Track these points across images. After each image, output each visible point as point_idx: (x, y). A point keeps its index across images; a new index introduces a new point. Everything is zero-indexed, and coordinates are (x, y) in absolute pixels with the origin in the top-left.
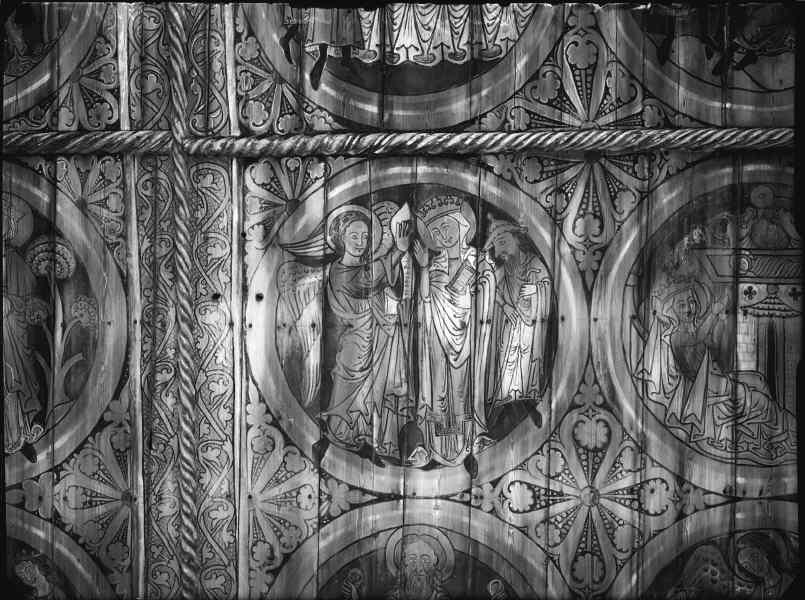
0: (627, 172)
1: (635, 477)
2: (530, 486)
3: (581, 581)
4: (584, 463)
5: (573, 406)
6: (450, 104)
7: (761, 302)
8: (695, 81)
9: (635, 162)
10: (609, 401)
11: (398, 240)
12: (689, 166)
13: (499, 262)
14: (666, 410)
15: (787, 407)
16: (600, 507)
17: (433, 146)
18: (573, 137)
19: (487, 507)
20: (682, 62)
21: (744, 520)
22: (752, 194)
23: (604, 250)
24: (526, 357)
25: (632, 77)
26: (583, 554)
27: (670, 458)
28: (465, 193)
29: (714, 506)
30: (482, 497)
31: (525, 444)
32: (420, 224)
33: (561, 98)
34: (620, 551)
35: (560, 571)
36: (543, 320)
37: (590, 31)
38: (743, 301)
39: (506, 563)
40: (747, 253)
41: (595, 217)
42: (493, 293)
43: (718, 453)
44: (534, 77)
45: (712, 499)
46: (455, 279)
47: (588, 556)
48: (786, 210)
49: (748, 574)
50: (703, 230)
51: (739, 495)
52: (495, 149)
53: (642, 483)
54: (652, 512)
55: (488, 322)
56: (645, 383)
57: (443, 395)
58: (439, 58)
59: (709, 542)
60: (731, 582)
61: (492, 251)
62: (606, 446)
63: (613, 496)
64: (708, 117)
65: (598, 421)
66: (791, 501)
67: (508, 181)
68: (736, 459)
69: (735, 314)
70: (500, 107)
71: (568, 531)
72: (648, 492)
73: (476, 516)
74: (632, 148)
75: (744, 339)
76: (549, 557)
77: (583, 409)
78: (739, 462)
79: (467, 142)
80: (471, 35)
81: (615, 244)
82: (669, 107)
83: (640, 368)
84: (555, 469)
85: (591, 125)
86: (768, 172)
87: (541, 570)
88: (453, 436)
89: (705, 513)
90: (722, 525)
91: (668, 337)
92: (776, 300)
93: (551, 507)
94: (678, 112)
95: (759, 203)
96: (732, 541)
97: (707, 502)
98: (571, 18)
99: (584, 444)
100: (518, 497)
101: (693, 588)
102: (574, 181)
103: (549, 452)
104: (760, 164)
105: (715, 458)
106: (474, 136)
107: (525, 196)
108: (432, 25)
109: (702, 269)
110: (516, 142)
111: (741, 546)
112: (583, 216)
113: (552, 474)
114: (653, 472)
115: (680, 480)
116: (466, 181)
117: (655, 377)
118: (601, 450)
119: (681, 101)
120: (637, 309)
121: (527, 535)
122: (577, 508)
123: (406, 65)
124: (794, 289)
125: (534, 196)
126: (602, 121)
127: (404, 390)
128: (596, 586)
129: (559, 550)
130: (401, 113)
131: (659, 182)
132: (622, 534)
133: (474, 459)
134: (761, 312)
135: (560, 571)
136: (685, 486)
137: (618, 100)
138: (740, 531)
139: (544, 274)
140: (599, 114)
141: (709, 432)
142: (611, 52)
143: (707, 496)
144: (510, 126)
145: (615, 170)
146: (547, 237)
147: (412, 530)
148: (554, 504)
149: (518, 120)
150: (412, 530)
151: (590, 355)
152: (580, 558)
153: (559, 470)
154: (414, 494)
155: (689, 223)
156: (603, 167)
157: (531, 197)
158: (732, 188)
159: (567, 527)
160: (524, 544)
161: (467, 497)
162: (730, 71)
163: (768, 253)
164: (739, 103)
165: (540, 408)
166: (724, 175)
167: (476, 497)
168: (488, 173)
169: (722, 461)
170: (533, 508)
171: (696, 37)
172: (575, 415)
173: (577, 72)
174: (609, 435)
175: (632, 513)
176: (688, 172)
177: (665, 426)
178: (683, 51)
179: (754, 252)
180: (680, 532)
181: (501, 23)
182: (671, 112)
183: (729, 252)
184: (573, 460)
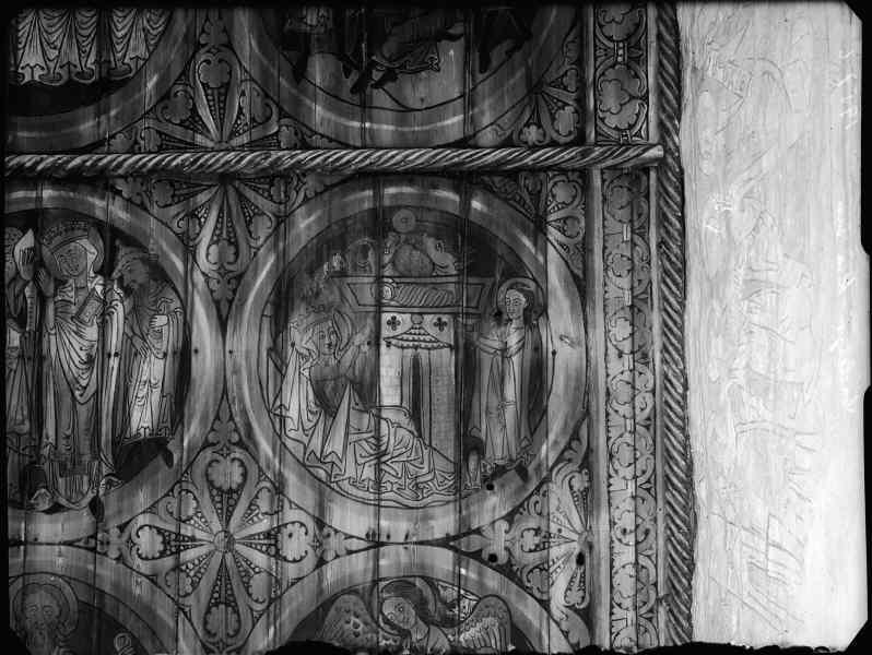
0: (262, 195)
1: (272, 520)
2: (159, 531)
3: (215, 635)
4: (219, 505)
5: (207, 445)
6: (79, 124)
7: (405, 333)
8: (333, 99)
9: (272, 185)
10: (244, 439)
11: (22, 269)
12: (327, 188)
13: (128, 291)
16: (236, 555)
17: (55, 167)
18: (199, 158)
19: (114, 554)
20: (318, 81)
21: (390, 566)
22: (394, 219)
23: (239, 277)
24: (157, 393)
25: (267, 96)
26: (216, 605)
27: (309, 500)
28: (93, 218)
29: (356, 552)
30: (108, 543)
31: (154, 485)
32: (46, 251)
33: (193, 118)
34: (257, 601)
35: (192, 624)
36: (174, 353)
37: (223, 48)
38: (386, 332)
39: (133, 615)
40: (391, 281)
41: (230, 243)
42: (121, 326)
43: (360, 494)
44: (164, 96)
45: (355, 544)
46: (81, 310)
47: (222, 607)
48: (429, 236)
49: (393, 626)
50: (343, 256)
51: (383, 539)
52: (120, 171)
53: (279, 527)
55: (116, 354)
56: (283, 419)
57: (69, 432)
58: (65, 77)
59: (352, 591)
60: (375, 635)
61: (121, 279)
62: (241, 486)
63: (249, 541)
64: (347, 136)
65: (233, 460)
66: (438, 545)
67: (137, 206)
68: (380, 500)
69: (378, 345)
70: (129, 128)
72: (286, 537)
73: (101, 563)
74: (263, 170)
75: (387, 372)
76: (180, 608)
77: (218, 447)
78: (383, 503)
79: (88, 164)
80: (99, 54)
81: (250, 274)
82: (307, 127)
83: (278, 403)
84: (186, 511)
85: (224, 145)
86: (411, 195)
88: (78, 476)
89: (348, 557)
90: (365, 571)
91: (307, 370)
92: (422, 332)
93: (182, 554)
94: (316, 133)
95: (401, 227)
96: (375, 590)
97: (349, 547)
98: (204, 35)
99: (217, 484)
100: (147, 542)
102: (208, 205)
104: (402, 185)
105: (357, 500)
106: (95, 157)
107: (155, 221)
108: (58, 44)
109: (342, 296)
110: (140, 163)
111: (385, 595)
112: (217, 242)
113: (184, 518)
114: (291, 515)
115: (320, 523)
116: (93, 205)
117: (293, 413)
118: (236, 492)
119: (318, 119)
120: (275, 341)
122: (210, 554)
123: (32, 84)
124: (439, 319)
125: (164, 221)
126: (236, 142)
127: (26, 427)
128: (230, 641)
129: (190, 601)
130: (26, 134)
131: (295, 206)
132: (258, 584)
133: (100, 501)
134: (405, 344)
135: (192, 624)
136: (326, 530)
137: (253, 119)
138: (385, 579)
139: (179, 304)
140: (233, 134)
141: (351, 472)
142: (246, 71)
143: (349, 540)
144: (140, 148)
145: (250, 194)
146: (180, 265)
149: (148, 139)
150: (32, 579)
151: (225, 391)
152: (214, 609)
154: (36, 539)
155: (329, 249)
156: (237, 190)
157: (161, 221)
158: (374, 211)
159: (200, 575)
160: (153, 592)
162: (369, 89)
163: (413, 280)
164: (379, 122)
165: (171, 446)
166: (364, 198)
167: (102, 543)
168: (117, 198)
169: (364, 502)
170: (163, 554)
171: (333, 54)
172: (208, 454)
173: (209, 92)
174: (245, 475)
176: (326, 196)
177: (304, 465)
178: (320, 70)
179: (397, 280)
180: (320, 581)
181: (133, 37)
182: (309, 133)
183: (372, 280)
184: (206, 500)
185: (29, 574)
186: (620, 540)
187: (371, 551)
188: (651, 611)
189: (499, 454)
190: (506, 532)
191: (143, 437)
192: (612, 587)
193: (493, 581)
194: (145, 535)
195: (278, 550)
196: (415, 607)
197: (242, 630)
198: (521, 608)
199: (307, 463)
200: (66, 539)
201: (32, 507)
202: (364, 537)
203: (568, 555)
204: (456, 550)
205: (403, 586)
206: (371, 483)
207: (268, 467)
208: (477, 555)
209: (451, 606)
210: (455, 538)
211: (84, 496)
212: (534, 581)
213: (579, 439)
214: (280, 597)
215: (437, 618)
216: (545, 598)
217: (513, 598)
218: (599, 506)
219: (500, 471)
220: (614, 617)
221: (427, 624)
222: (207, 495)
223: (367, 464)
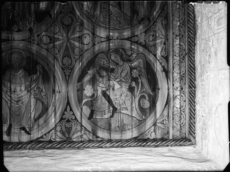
1: (80, 33)
2: (49, 37)
3: (65, 65)
4: (65, 29)
14: (89, 13)
15: (124, 12)
16: (70, 43)
19: (36, 42)
21: (113, 46)
26: (65, 57)
30: (34, 40)
34: (76, 56)
35: (59, 62)
45: (103, 40)
47: (67, 57)
49: (114, 62)
51: (111, 38)
54: (85, 44)
59: (102, 52)
63: (74, 39)
66: (126, 40)
71: (60, 50)
78: (111, 28)
87: (53, 62)
89: (101, 43)
90: (106, 47)
93: (55, 43)
96: (109, 52)
97: (101, 40)
99: (65, 24)
101: (98, 67)
103: (54, 26)
105: (103, 27)
111: (112, 53)
114: (86, 32)
115: (94, 34)
118: (70, 25)
121: (48, 51)
122: (63, 43)
128: (69, 67)
129: (58, 55)
132: (77, 51)
133: (32, 29)
136: (95, 36)
138: (111, 49)
143: (101, 39)
147: (13, 50)
148: (56, 41)
150: (13, 50)
152: (64, 58)
153: (58, 31)
154: (14, 39)
160: (47, 54)
161: (30, 40)
165: (51, 13)
167: (33, 40)
170: (50, 43)
172: (62, 15)
174: (72, 21)
175: (79, 44)
180: (94, 49)
185: (12, 49)
186: (175, 38)
188: (183, 57)
189: (142, 15)
190: (145, 36)
191: (43, 10)
192: (173, 51)
193: (141, 49)
194: (44, 38)
195: (82, 41)
196: (120, 57)
197: (72, 64)
198: (149, 56)
199: (89, 17)
200: (22, 39)
201: (13, 30)
202: (106, 38)
203: (161, 42)
204: (131, 41)
205: (116, 51)
206: (108, 23)
207: (79, 18)
208: (136, 42)
209: (130, 56)
210: (131, 38)
211: (27, 27)
212: (152, 49)
213: (164, 10)
214: (83, 54)
215: (126, 59)
216: (155, 54)
217: (146, 54)
218: (170, 28)
219: (143, 19)
220: (174, 59)
222: (62, 27)
223: (106, 18)
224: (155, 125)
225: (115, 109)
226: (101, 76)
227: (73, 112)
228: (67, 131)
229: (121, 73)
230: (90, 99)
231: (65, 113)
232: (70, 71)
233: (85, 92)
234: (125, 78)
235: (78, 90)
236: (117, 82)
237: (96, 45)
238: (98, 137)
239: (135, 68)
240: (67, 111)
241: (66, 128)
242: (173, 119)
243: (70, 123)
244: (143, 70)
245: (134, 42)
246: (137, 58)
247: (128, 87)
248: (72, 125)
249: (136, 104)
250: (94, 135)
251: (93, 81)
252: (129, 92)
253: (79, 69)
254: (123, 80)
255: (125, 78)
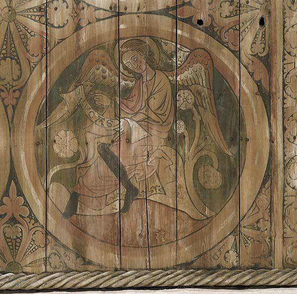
3: (4, 79)
34: (33, 55)
45: (101, 14)
59: (100, 47)
66: (161, 14)
89: (97, 24)
101: (88, 83)
111: (124, 49)
132: (34, 43)
136: (81, 5)
138: (123, 39)
175: (41, 26)
180: (78, 40)
186: (290, 8)
187: (114, 19)
193: (200, 37)
195: (47, 19)
197: (22, 76)
203: (252, 19)
205: (136, 43)
209: (170, 56)
210: (173, 8)
216: (237, 49)
217: (214, 51)
220: (285, 62)
221: (154, 69)
224: (236, 231)
225: (132, 192)
226: (97, 108)
227: (25, 199)
228: (9, 246)
229: (148, 99)
230: (68, 166)
231: (5, 200)
232: (17, 94)
233: (56, 148)
234: (159, 112)
235: (37, 144)
236: (137, 122)
237: (82, 27)
238: (90, 263)
239: (185, 87)
240: (8, 196)
241: (8, 238)
242: (284, 216)
243: (16, 227)
244: (205, 92)
245: (183, 20)
246: (190, 60)
247: (165, 136)
248: (21, 232)
249: (186, 180)
250: (78, 256)
251: (77, 122)
252: (168, 148)
253: (40, 89)
254: (153, 116)
255: (159, 112)
